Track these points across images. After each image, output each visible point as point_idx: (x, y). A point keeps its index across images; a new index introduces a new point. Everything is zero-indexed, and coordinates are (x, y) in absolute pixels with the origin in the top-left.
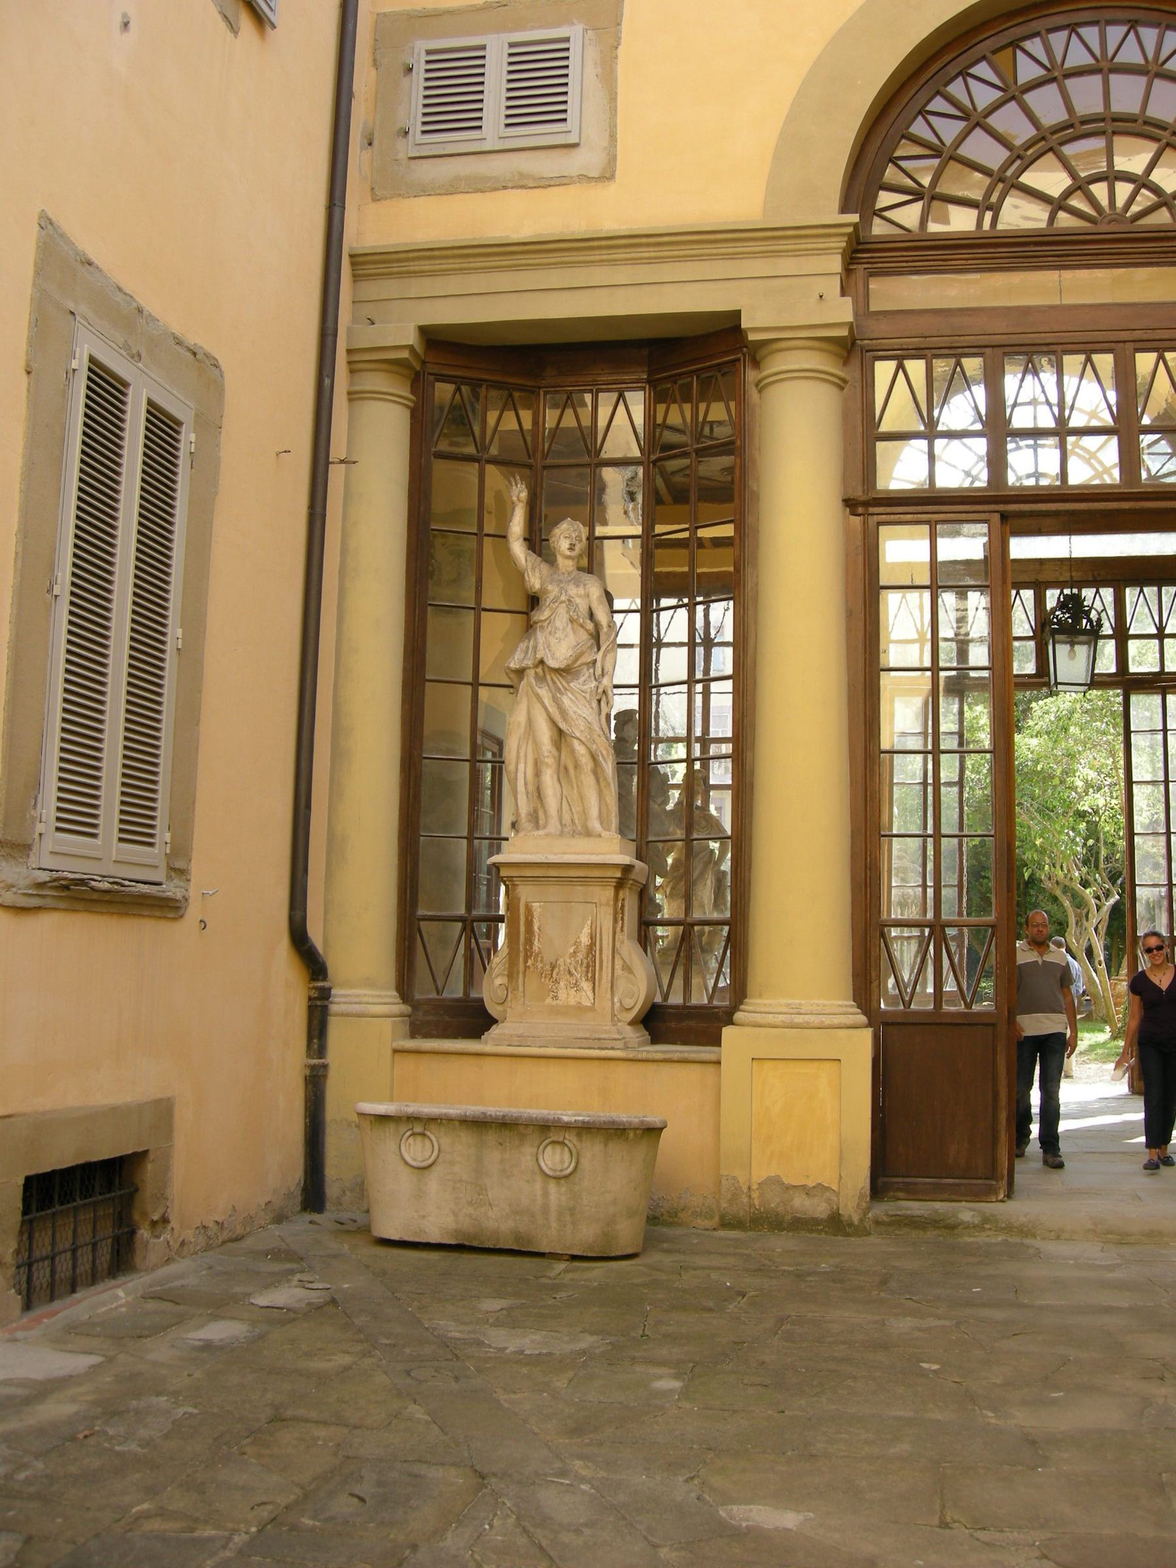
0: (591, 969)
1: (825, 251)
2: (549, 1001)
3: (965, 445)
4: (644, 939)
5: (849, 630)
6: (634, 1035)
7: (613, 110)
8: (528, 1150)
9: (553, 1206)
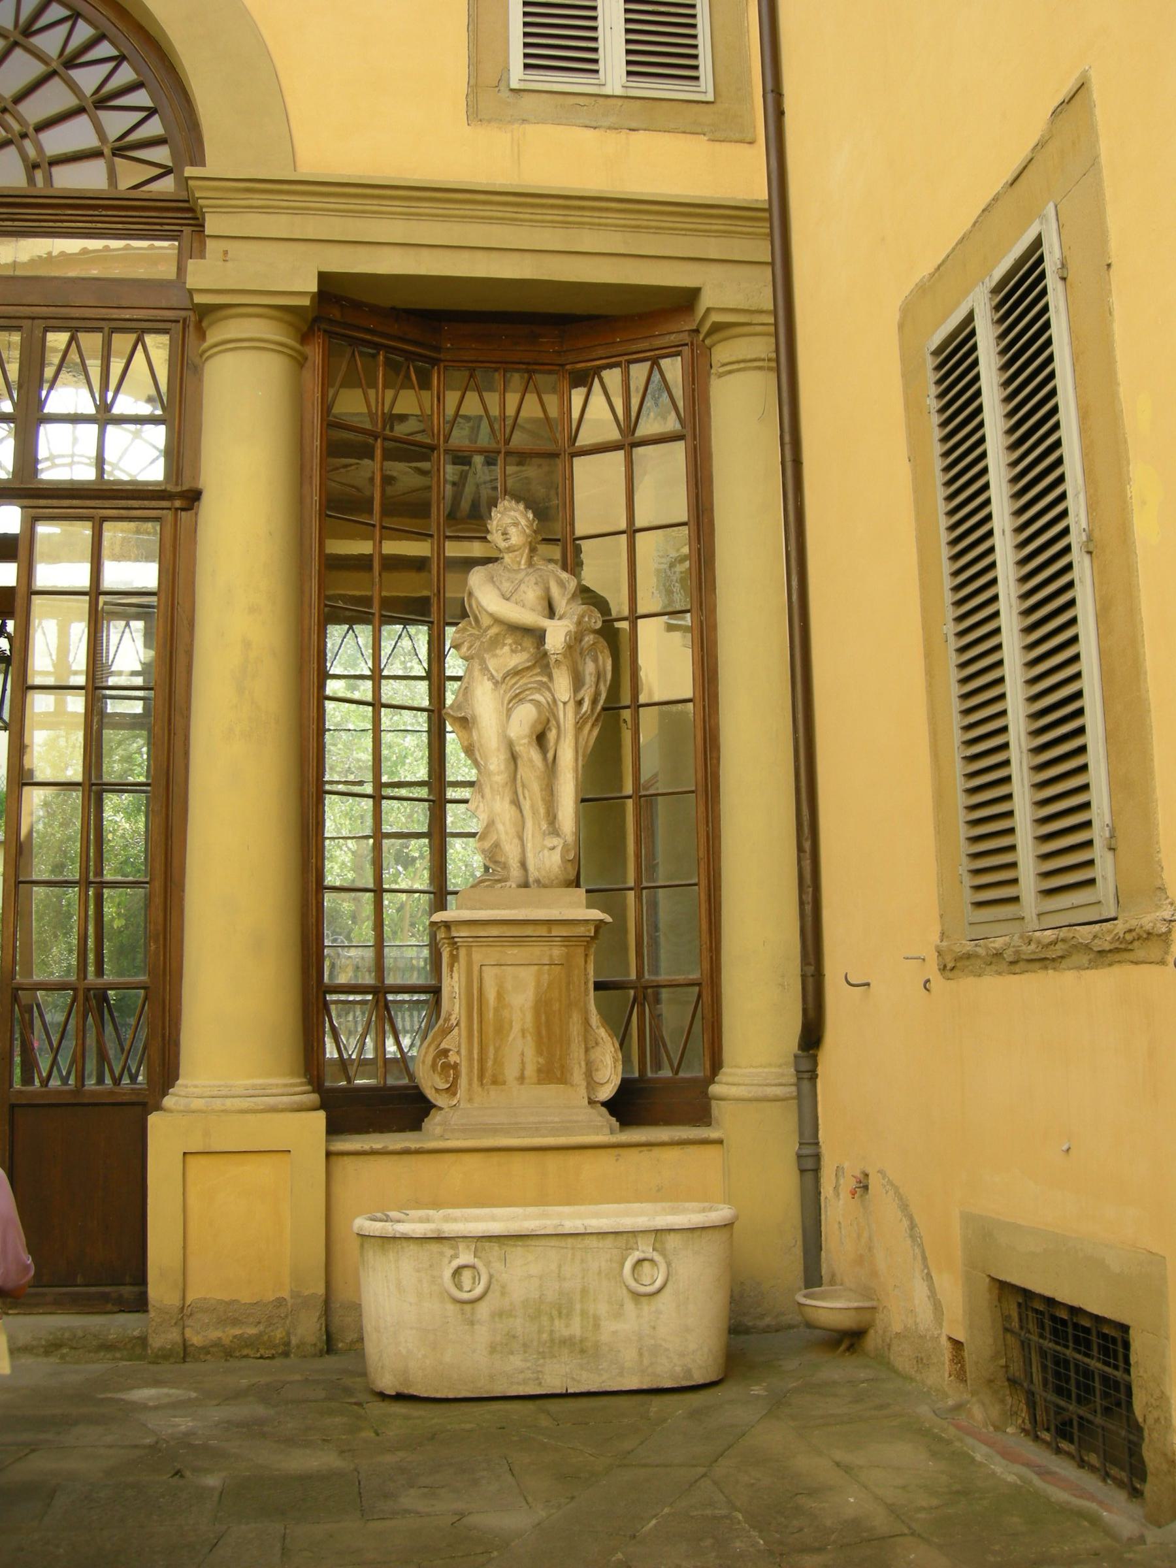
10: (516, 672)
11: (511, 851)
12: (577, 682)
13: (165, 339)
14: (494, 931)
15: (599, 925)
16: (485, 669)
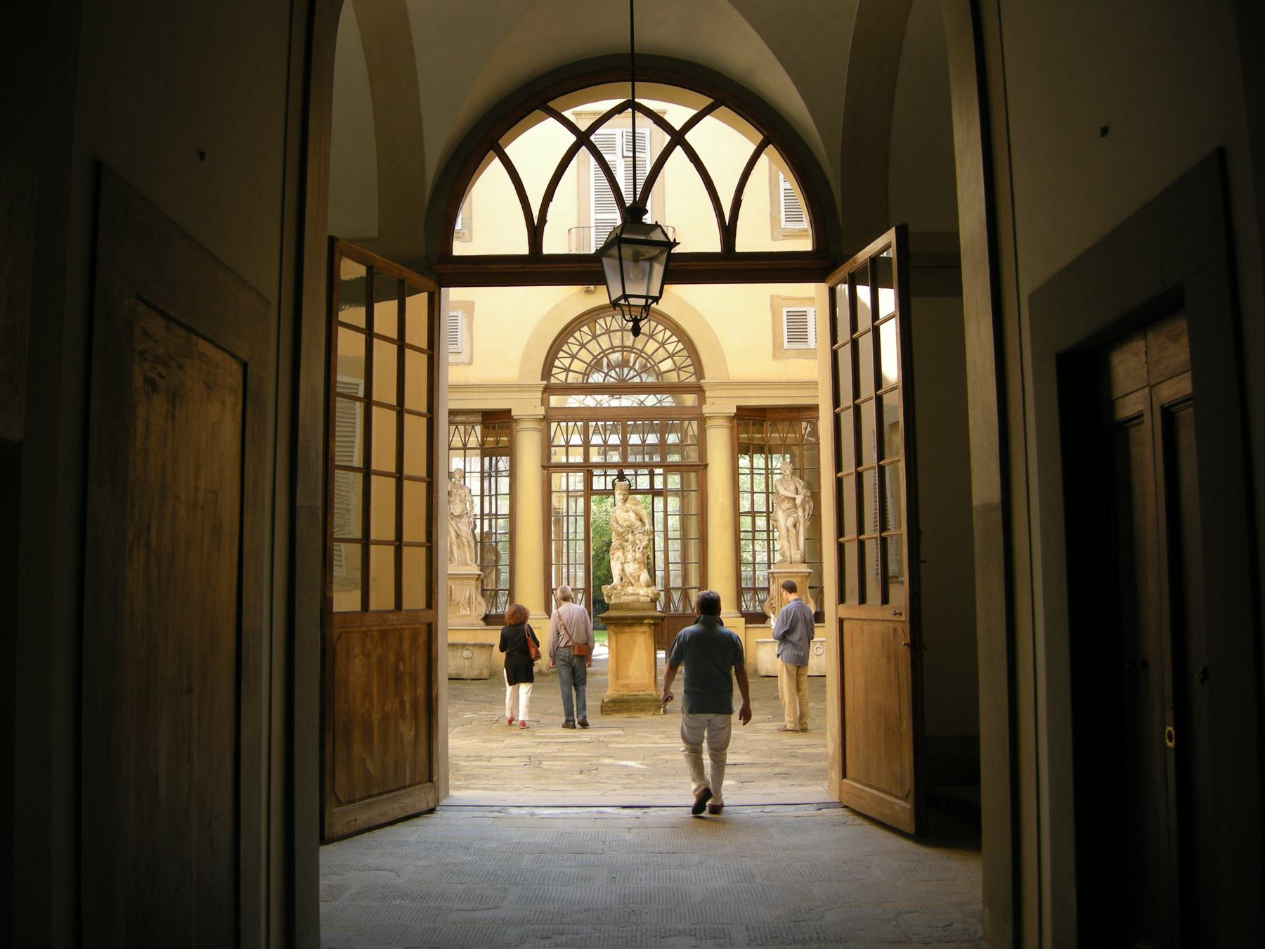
0: (469, 604)
1: (537, 391)
2: (457, 614)
3: (594, 399)
4: (483, 595)
5: (543, 504)
6: (482, 623)
7: (472, 341)
8: (459, 652)
9: (466, 667)
10: (788, 509)
11: (787, 554)
12: (804, 510)
13: (696, 422)
14: (784, 574)
15: (810, 573)
16: (780, 507)
